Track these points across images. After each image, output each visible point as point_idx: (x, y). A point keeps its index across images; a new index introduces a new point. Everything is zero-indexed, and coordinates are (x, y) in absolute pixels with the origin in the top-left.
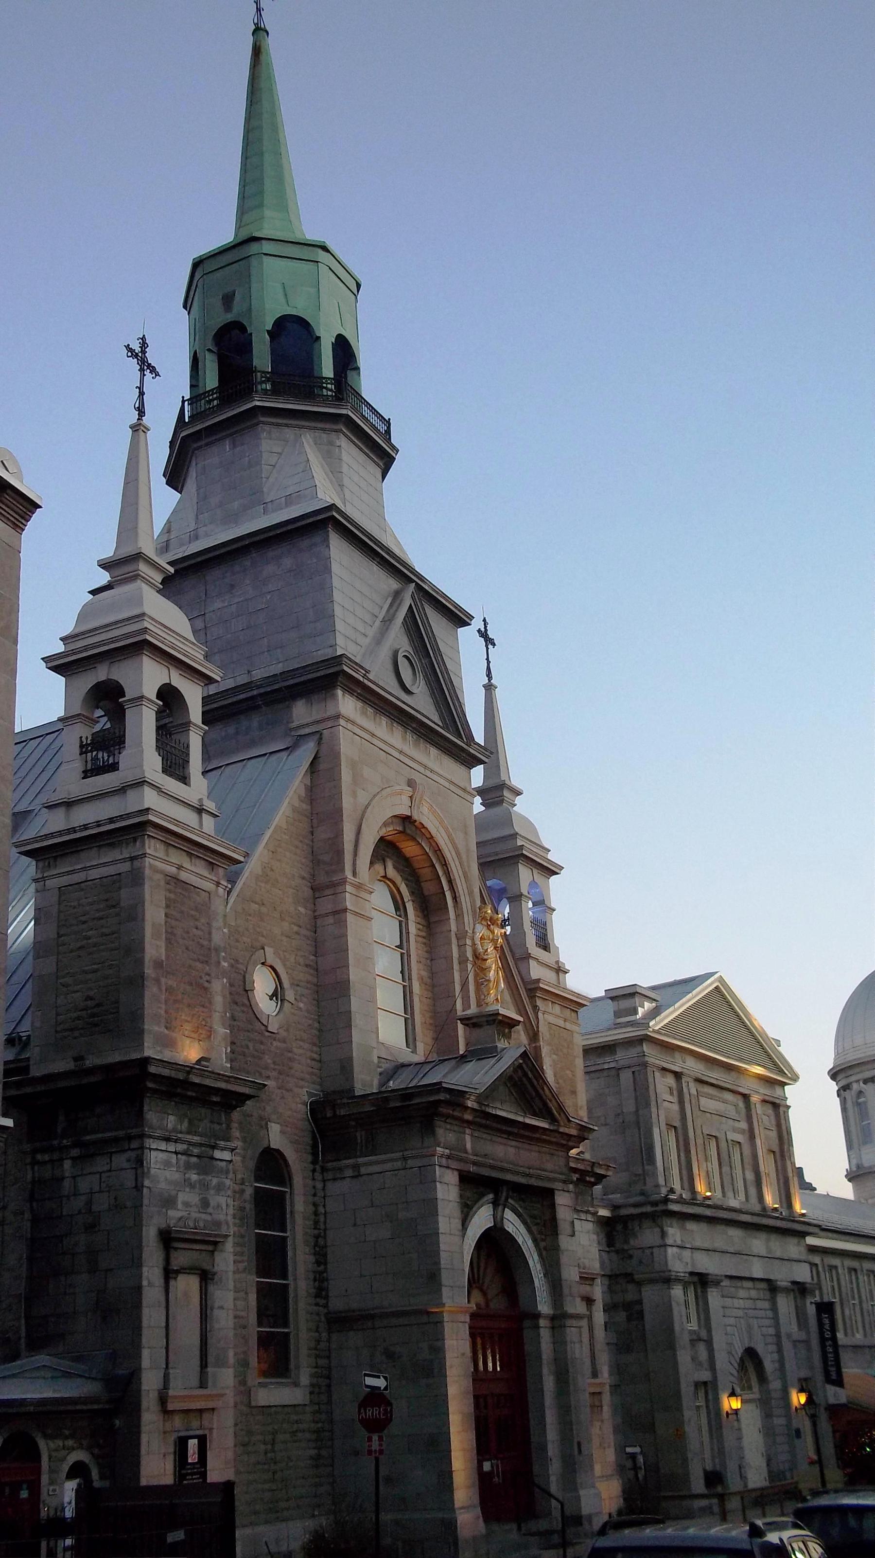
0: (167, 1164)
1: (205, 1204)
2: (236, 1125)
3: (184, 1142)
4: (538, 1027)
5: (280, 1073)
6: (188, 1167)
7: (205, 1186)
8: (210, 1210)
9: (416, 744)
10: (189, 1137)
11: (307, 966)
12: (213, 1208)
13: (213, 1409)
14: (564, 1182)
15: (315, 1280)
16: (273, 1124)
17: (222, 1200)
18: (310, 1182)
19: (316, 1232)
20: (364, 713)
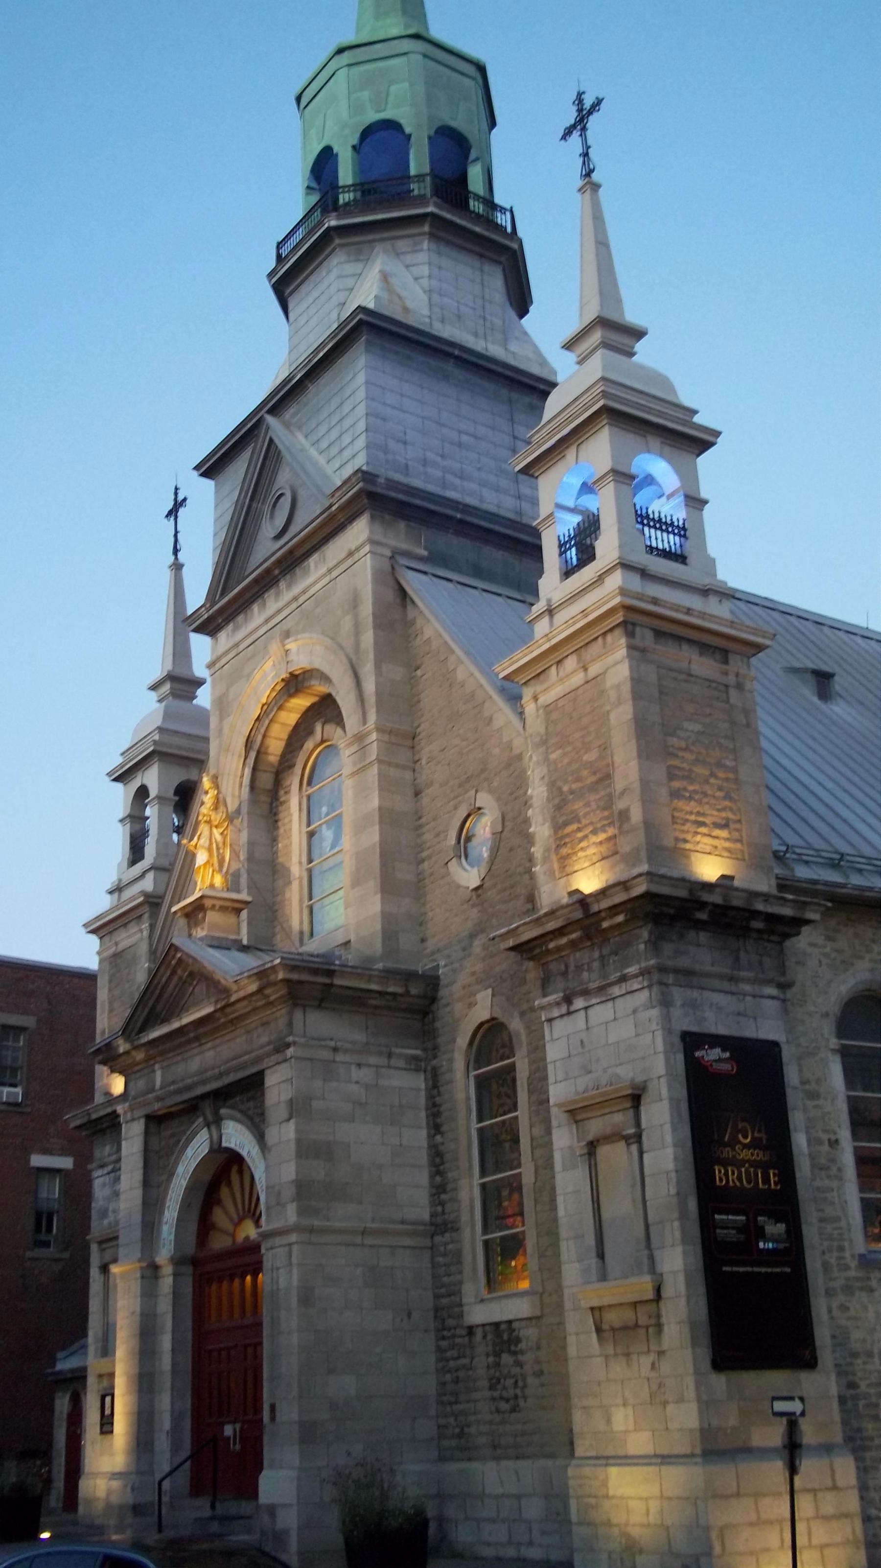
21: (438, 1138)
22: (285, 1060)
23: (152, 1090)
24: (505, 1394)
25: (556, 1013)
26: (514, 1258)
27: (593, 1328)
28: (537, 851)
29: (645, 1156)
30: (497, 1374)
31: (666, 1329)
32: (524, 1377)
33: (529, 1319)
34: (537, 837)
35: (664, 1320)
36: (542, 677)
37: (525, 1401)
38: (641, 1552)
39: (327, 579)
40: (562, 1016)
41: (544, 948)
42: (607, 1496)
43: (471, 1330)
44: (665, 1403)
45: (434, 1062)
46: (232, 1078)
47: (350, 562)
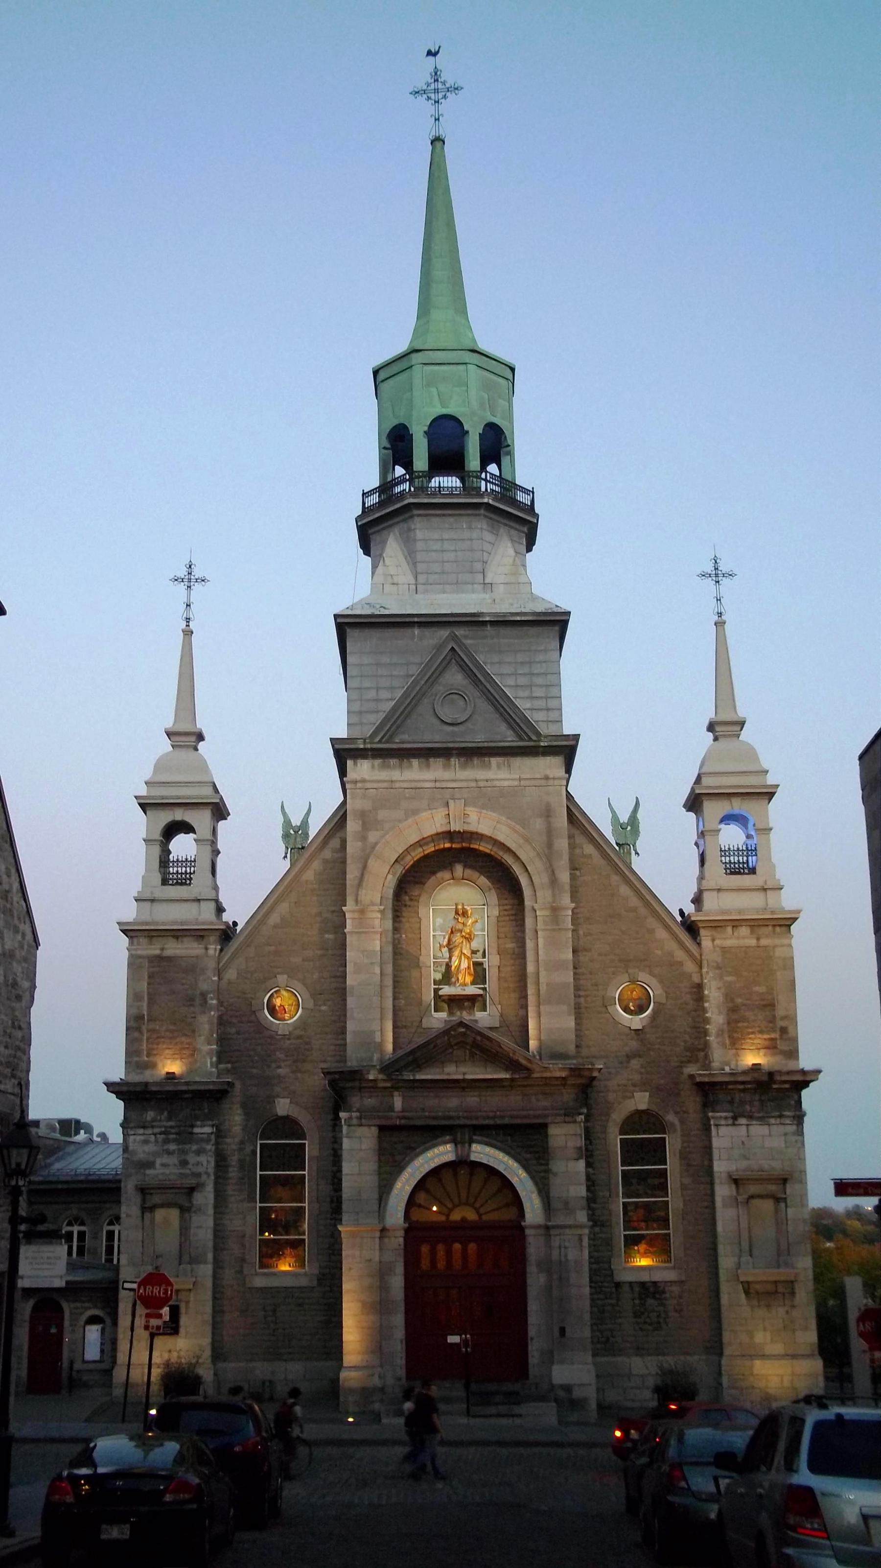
0: (146, 1142)
1: (184, 1163)
2: (238, 1106)
3: (160, 1127)
4: (701, 955)
5: (295, 1061)
6: (166, 1141)
7: (184, 1152)
8: (190, 1166)
9: (463, 767)
10: (165, 1123)
11: (335, 977)
12: (193, 1165)
13: (190, 1290)
14: (565, 1115)
15: (332, 1201)
16: (282, 1100)
17: (203, 1159)
18: (331, 1135)
19: (335, 1169)
20: (384, 767)
21: (590, 1170)
22: (575, 1122)
23: (391, 1109)
24: (648, 1320)
25: (723, 1122)
26: (637, 1245)
27: (742, 1291)
28: (712, 1028)
29: (789, 1210)
30: (642, 1310)
31: (797, 1295)
32: (666, 1312)
33: (675, 1282)
34: (712, 1020)
35: (797, 1291)
36: (719, 929)
37: (667, 1325)
38: (776, 1400)
39: (516, 783)
40: (727, 1125)
41: (724, 1087)
42: (752, 1375)
43: (618, 1285)
44: (794, 1331)
45: (589, 1124)
46: (507, 1121)
47: (543, 782)
